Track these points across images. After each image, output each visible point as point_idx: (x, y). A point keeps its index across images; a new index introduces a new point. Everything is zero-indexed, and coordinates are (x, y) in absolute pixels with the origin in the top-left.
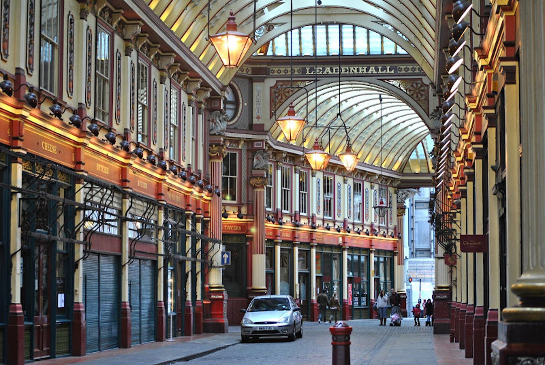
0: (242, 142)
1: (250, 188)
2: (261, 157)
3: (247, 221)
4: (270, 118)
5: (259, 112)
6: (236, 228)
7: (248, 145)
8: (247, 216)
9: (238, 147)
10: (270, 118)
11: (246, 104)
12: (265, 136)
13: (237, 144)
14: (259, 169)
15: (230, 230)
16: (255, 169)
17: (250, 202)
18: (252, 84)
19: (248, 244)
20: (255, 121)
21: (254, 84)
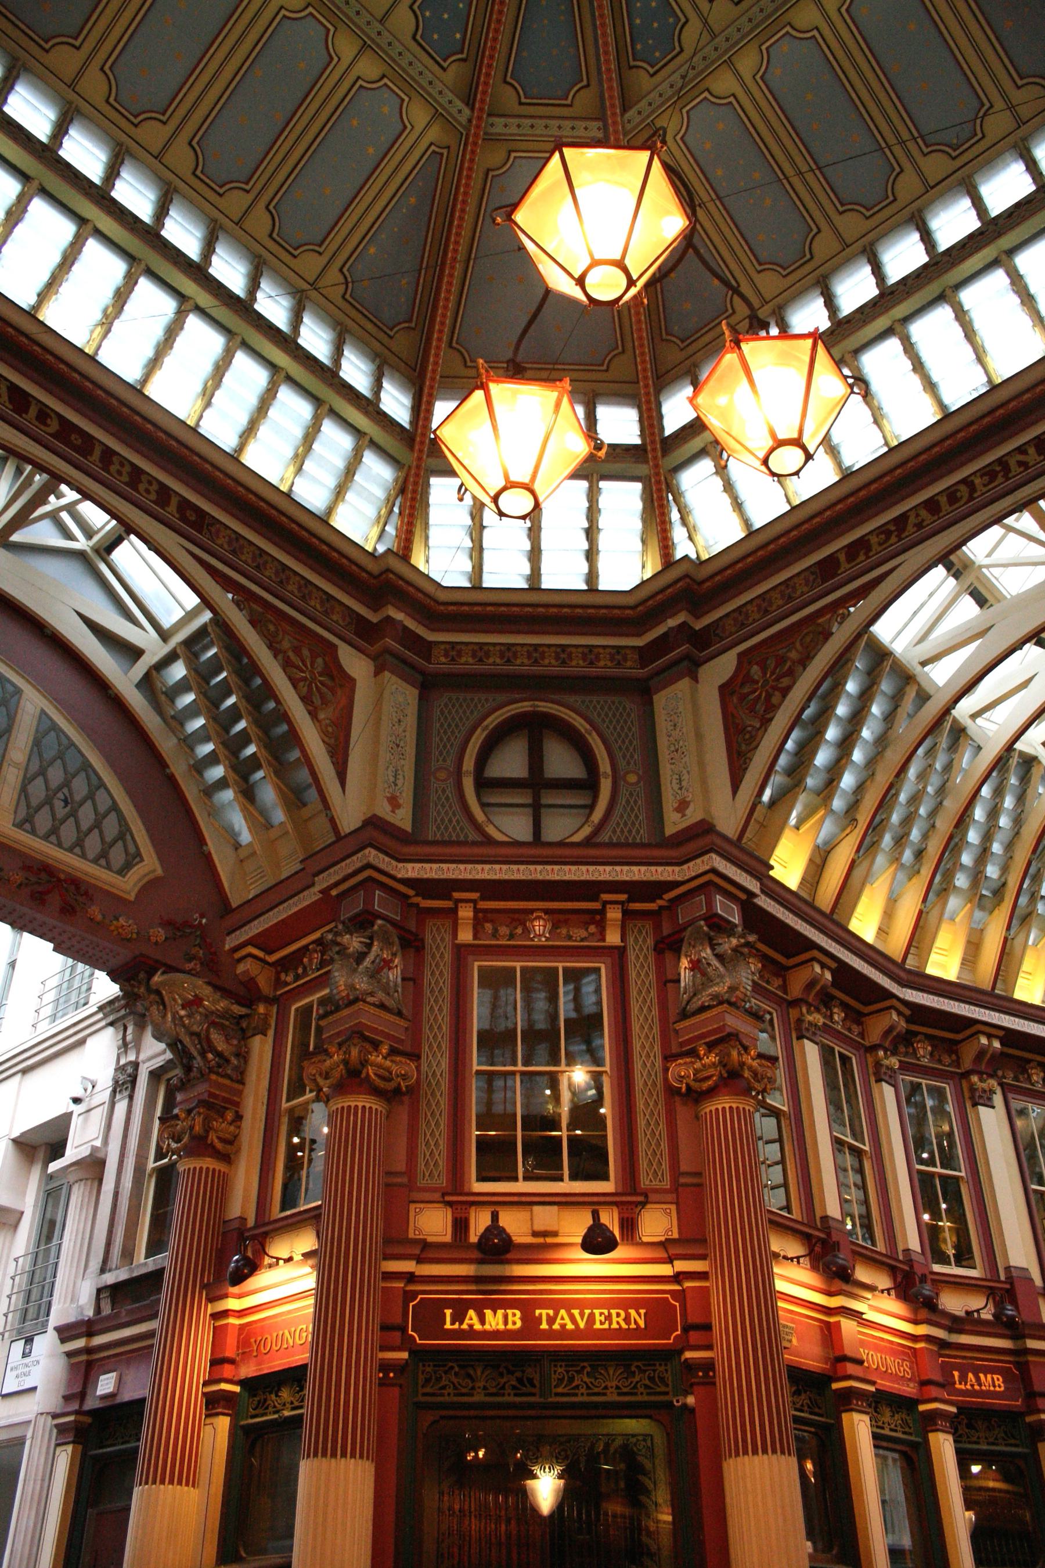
0: (614, 914)
1: (683, 1112)
2: (707, 953)
3: (678, 1277)
4: (735, 788)
5: (684, 783)
6: (609, 1318)
7: (657, 927)
8: (667, 1250)
9: (604, 940)
10: (735, 788)
11: (632, 778)
12: (706, 858)
13: (592, 929)
14: (703, 1009)
15: (577, 1333)
16: (684, 1015)
17: (682, 1180)
18: (651, 703)
19: (691, 1400)
20: (674, 823)
21: (660, 700)
